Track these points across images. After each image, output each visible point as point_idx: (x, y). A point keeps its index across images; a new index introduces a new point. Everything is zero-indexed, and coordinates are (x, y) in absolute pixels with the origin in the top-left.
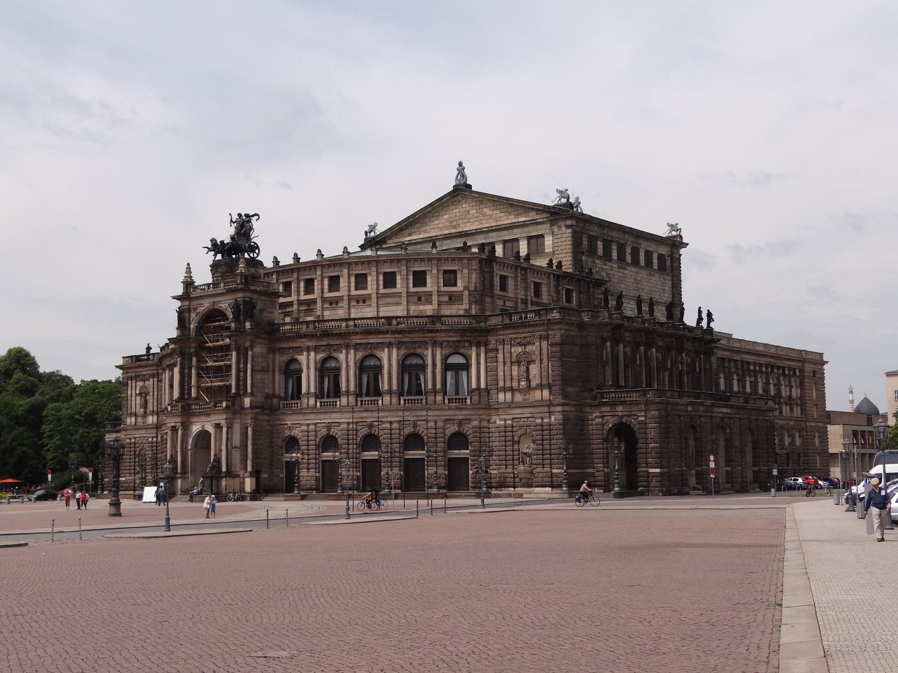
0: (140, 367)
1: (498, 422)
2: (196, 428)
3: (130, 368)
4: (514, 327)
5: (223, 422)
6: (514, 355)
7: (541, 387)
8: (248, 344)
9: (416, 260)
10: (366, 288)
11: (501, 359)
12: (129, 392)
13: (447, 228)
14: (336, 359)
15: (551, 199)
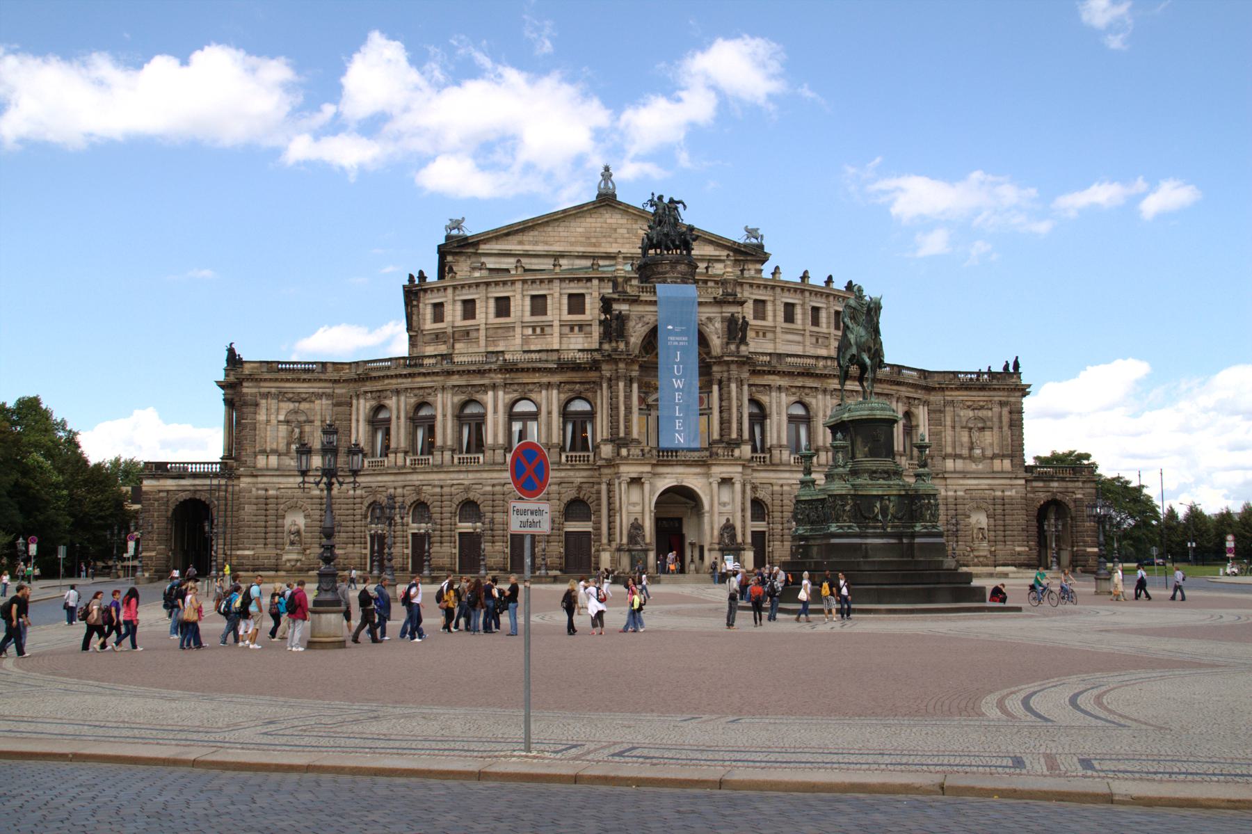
0: (298, 380)
1: (943, 493)
2: (663, 484)
3: (265, 380)
4: (970, 389)
5: (738, 480)
6: (964, 419)
7: (1003, 457)
8: (745, 375)
9: (816, 293)
10: (764, 318)
11: (949, 423)
12: (262, 417)
13: (582, 244)
14: (806, 406)
15: (739, 237)
